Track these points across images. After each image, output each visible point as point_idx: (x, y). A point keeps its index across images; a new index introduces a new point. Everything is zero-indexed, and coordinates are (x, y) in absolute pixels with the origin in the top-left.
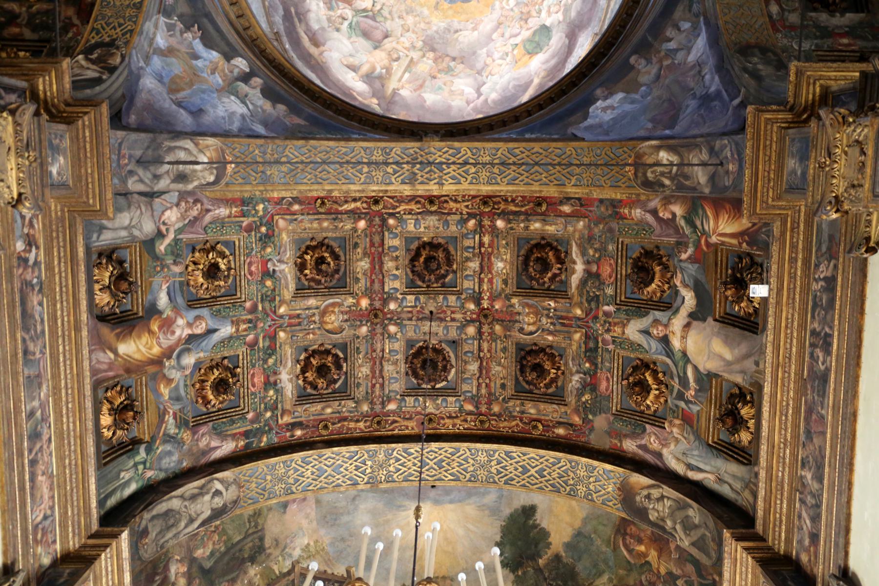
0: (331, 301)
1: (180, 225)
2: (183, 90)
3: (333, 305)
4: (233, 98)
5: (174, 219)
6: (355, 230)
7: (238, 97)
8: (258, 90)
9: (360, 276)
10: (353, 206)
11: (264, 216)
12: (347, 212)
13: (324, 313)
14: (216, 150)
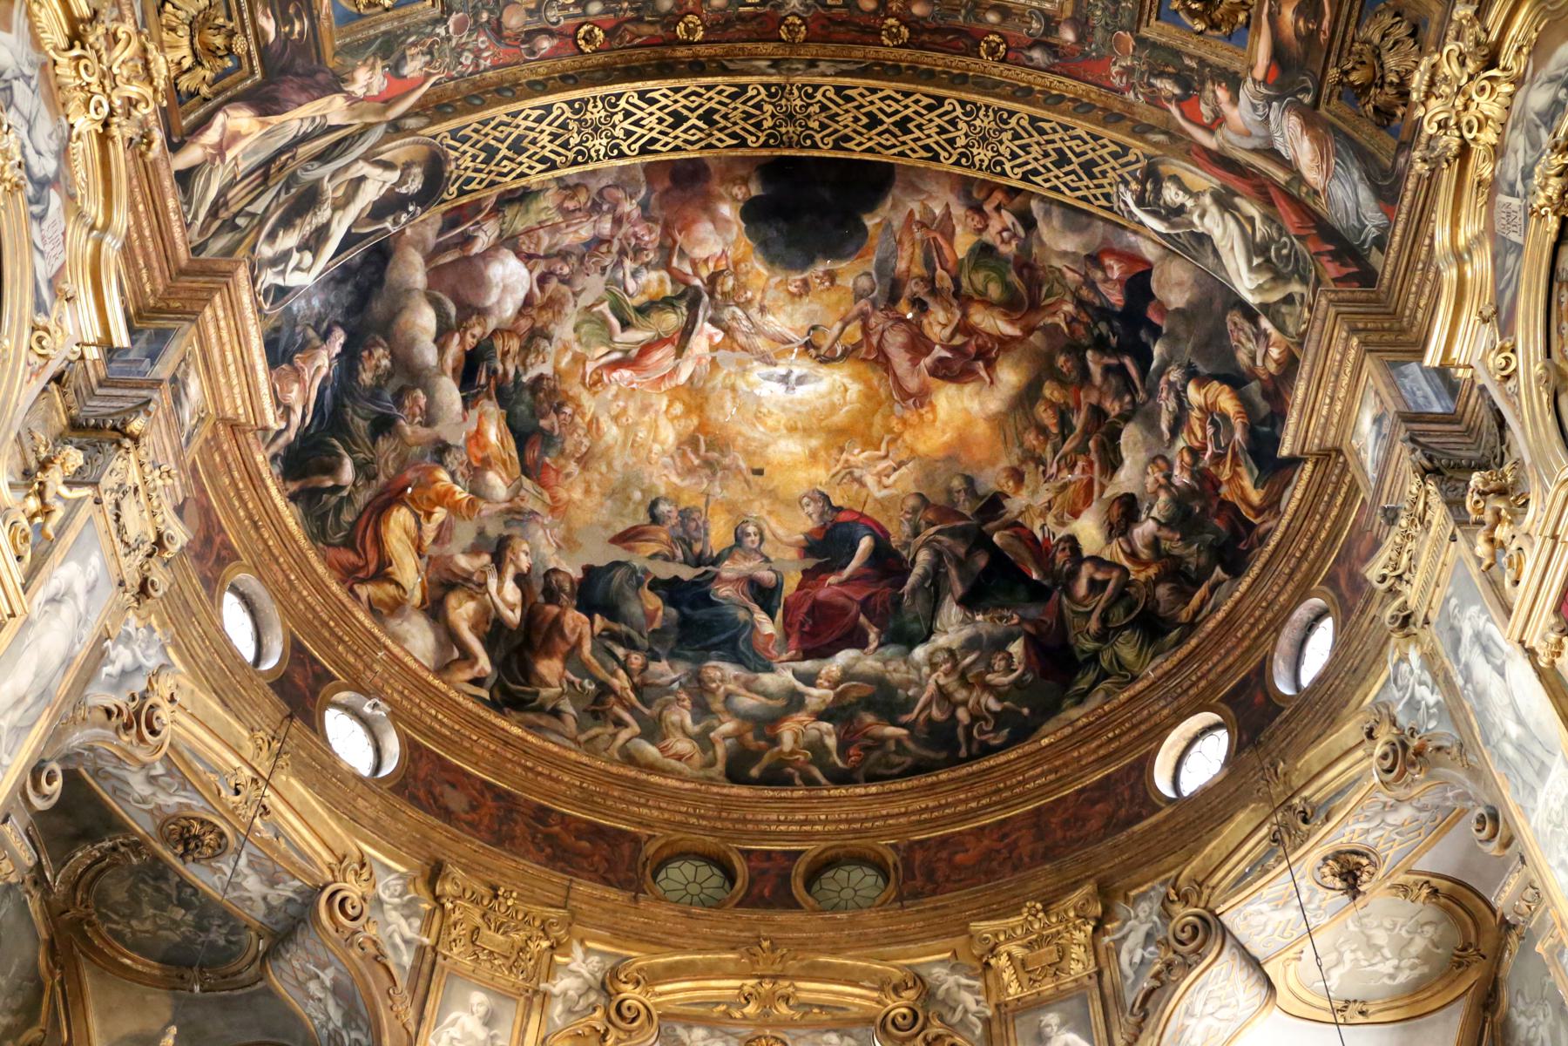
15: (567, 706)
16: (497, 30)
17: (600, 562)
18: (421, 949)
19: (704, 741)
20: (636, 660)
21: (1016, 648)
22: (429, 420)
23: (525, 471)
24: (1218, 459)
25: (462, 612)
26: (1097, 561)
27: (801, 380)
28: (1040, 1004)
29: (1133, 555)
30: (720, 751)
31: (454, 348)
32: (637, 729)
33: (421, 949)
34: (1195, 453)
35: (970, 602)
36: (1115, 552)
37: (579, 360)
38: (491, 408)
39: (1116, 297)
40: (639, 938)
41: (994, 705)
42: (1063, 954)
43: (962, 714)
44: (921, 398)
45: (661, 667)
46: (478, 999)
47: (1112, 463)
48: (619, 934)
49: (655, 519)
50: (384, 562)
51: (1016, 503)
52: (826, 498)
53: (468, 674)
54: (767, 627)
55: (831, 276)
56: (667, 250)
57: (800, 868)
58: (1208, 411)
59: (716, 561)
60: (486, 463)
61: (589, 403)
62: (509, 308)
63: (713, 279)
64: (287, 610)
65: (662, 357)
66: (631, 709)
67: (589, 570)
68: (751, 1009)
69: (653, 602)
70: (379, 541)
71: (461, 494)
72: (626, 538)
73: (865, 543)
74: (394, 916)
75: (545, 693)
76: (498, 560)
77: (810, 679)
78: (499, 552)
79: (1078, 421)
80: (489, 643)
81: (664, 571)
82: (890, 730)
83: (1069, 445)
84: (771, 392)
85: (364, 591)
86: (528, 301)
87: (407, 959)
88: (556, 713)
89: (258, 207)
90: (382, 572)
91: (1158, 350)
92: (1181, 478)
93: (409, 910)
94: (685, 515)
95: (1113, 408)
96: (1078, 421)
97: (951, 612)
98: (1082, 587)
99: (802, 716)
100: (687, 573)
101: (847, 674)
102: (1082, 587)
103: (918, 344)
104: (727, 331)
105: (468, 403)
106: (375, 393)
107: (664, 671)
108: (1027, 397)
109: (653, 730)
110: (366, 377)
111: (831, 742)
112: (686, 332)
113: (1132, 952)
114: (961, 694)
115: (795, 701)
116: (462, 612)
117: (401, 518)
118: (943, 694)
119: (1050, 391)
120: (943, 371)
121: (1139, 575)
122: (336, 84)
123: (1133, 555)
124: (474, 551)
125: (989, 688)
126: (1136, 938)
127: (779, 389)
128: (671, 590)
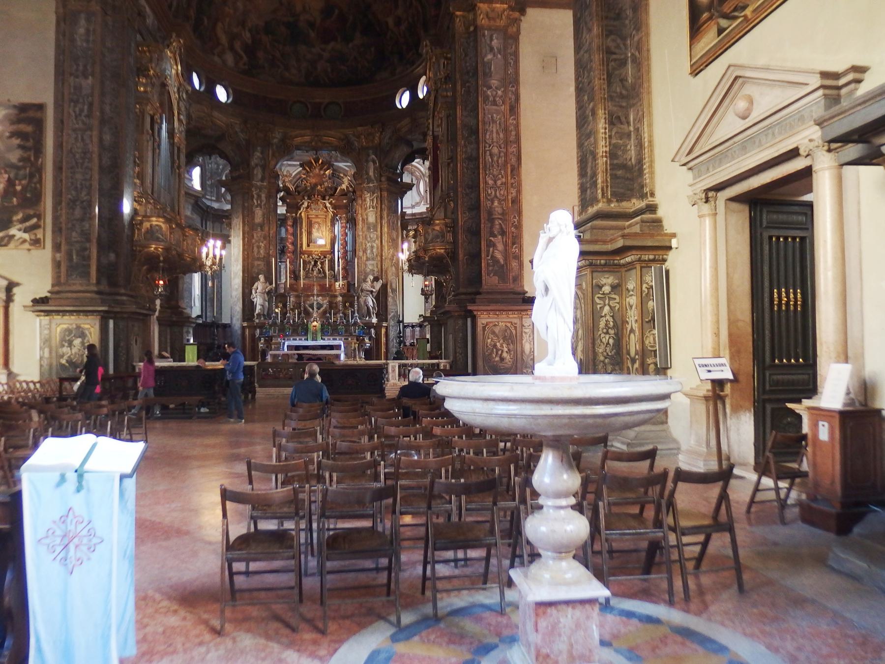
21: (373, 49)
25: (238, 45)
42: (374, 138)
54: (313, 35)
68: (313, 143)
73: (337, 11)
77: (324, 50)
78: (243, 24)
87: (244, 143)
111: (329, 70)
116: (238, 45)
117: (220, 25)
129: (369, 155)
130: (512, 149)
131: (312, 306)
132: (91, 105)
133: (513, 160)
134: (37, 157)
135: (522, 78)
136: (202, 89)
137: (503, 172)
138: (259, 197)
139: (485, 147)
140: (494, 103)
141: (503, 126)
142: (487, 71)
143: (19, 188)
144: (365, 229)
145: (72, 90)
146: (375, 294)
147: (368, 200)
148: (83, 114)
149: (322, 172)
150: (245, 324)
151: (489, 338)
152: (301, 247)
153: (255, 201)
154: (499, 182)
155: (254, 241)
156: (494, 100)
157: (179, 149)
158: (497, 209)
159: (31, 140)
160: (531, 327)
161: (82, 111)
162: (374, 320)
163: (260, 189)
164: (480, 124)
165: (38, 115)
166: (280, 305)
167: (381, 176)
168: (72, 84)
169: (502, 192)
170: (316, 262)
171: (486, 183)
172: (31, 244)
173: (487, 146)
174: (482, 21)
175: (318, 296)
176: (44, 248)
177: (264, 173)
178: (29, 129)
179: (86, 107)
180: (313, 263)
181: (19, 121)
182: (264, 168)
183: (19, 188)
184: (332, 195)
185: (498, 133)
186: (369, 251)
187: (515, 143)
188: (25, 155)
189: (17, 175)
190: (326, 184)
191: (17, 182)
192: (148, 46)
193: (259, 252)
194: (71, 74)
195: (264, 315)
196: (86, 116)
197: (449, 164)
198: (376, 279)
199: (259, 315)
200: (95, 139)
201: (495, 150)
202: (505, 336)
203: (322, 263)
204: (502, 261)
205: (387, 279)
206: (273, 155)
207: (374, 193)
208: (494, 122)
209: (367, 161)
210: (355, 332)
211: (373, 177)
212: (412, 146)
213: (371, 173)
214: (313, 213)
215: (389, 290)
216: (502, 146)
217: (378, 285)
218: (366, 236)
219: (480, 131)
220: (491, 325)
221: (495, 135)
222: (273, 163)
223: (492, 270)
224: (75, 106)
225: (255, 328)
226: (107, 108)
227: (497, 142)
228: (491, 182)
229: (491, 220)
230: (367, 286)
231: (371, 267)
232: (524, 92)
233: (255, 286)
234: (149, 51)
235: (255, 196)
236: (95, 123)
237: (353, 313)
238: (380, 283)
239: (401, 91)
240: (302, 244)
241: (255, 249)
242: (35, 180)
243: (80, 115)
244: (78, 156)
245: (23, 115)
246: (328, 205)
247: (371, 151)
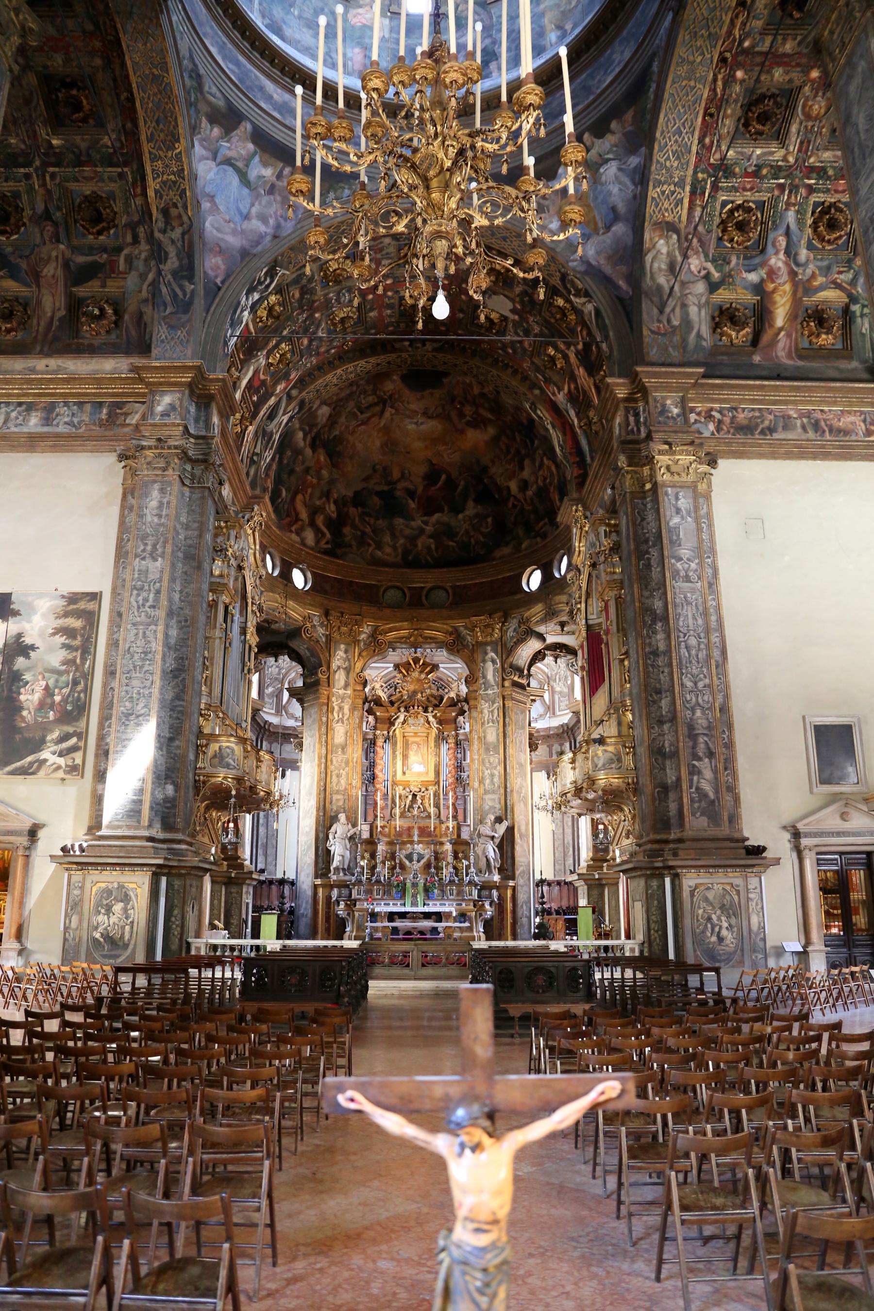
0: (800, 109)
1: (702, 255)
2: (594, 217)
3: (804, 106)
4: (602, 170)
5: (697, 262)
6: (743, 81)
7: (601, 165)
8: (595, 140)
9: (787, 78)
10: (720, 83)
11: (708, 172)
12: (724, 89)
13: (808, 116)
14: (654, 230)
15: (354, 543)
16: (318, 354)
17: (358, 489)
18: (327, 636)
19: (394, 547)
20: (372, 521)
21: (490, 520)
22: (303, 463)
23: (333, 465)
24: (550, 484)
26: (515, 497)
27: (422, 424)
28: (486, 644)
29: (525, 500)
30: (400, 551)
31: (309, 438)
32: (374, 546)
33: (327, 636)
34: (545, 479)
35: (477, 501)
36: (520, 496)
37: (347, 427)
38: (321, 451)
39: (525, 421)
40: (380, 619)
41: (482, 539)
43: (472, 540)
44: (462, 432)
45: (380, 522)
46: (342, 646)
47: (522, 468)
48: (375, 618)
49: (375, 470)
50: (297, 514)
51: (493, 470)
52: (430, 461)
53: (324, 541)
54: (413, 505)
55: (432, 394)
56: (374, 392)
57: (424, 593)
58: (549, 468)
59: (396, 483)
60: (321, 468)
61: (351, 438)
62: (324, 420)
63: (391, 396)
64: (280, 552)
65: (375, 420)
66: (372, 539)
67: (356, 493)
69: (376, 500)
70: (295, 509)
71: (315, 481)
72: (367, 479)
73: (444, 477)
74: (319, 628)
75: (347, 539)
76: (328, 499)
77: (426, 523)
78: (327, 495)
79: (513, 451)
80: (328, 527)
81: (378, 488)
82: (451, 543)
83: (509, 457)
84: (410, 427)
85: (293, 529)
86: (330, 416)
88: (350, 546)
89: (258, 450)
90: (297, 519)
91: (536, 442)
92: (540, 483)
93: (322, 625)
94: (385, 468)
95: (523, 452)
96: (513, 451)
97: (470, 504)
98: (510, 505)
99: (424, 537)
100: (386, 488)
101: (438, 522)
102: (510, 505)
103: (461, 415)
104: (397, 410)
105: (314, 452)
106: (288, 464)
107: (381, 523)
108: (496, 439)
109: (379, 546)
110: (285, 462)
111: (433, 546)
112: (382, 412)
113: (510, 633)
114: (472, 533)
115: (422, 531)
116: (320, 520)
117: (300, 497)
118: (467, 532)
119: (504, 438)
120: (469, 424)
121: (528, 508)
122: (272, 395)
123: (525, 500)
124: (320, 498)
125: (481, 533)
126: (511, 629)
127: (414, 426)
128: (381, 494)
129: (486, 653)
130: (715, 638)
131: (409, 857)
132: (158, 592)
133: (716, 653)
134: (84, 659)
135: (719, 547)
136: (276, 573)
137: (705, 670)
138: (341, 708)
139: (678, 637)
140: (687, 579)
141: (701, 608)
142: (675, 538)
143: (57, 698)
144: (482, 751)
145: (136, 576)
146: (497, 841)
147: (486, 711)
148: (148, 604)
149: (423, 676)
150: (318, 882)
151: (699, 908)
152: (395, 775)
153: (335, 714)
154: (701, 685)
155: (333, 767)
156: (687, 576)
157: (250, 647)
158: (700, 721)
159: (79, 638)
160: (758, 890)
161: (146, 600)
162: (496, 878)
163: (343, 699)
164: (670, 606)
165: (91, 606)
166: (367, 855)
167: (503, 680)
168: (137, 568)
169: (706, 698)
170: (414, 796)
171: (682, 685)
172: (66, 772)
173: (681, 635)
174: (663, 477)
175: (419, 842)
176: (82, 777)
177: (347, 677)
178: (77, 623)
179: (152, 596)
180: (410, 797)
181: (66, 615)
182: (348, 671)
183: (57, 698)
184: (436, 706)
185: (695, 618)
186: (487, 782)
187: (716, 630)
188: (70, 657)
189: (57, 681)
190: (428, 691)
191: (57, 691)
192: (226, 522)
193: (339, 782)
194: (136, 556)
195: (344, 869)
196: (150, 607)
197: (622, 661)
198: (499, 820)
199: (337, 869)
200: (160, 636)
201: (693, 641)
202: (724, 905)
203: (423, 798)
204: (712, 795)
205: (513, 819)
206: (360, 655)
207: (493, 703)
208: (689, 603)
209: (484, 661)
210: (471, 895)
211: (492, 682)
212: (544, 640)
213: (490, 676)
214: (410, 729)
215: (517, 835)
216: (702, 635)
217: (501, 829)
218: (483, 760)
219: (671, 616)
220: (702, 888)
221: (691, 621)
222: (359, 665)
223: (699, 808)
224: (138, 595)
225: (332, 887)
226: (177, 597)
227: (694, 631)
228: (689, 684)
229: (693, 737)
230: (486, 830)
231: (490, 804)
232: (723, 564)
233: (333, 830)
234: (226, 527)
235: (336, 708)
236: (161, 613)
237: (468, 867)
238: (505, 824)
239: (529, 570)
240: (395, 772)
241: (334, 777)
242: (80, 688)
243: (144, 605)
244: (136, 657)
245: (72, 607)
246: (431, 719)
247: (489, 648)
